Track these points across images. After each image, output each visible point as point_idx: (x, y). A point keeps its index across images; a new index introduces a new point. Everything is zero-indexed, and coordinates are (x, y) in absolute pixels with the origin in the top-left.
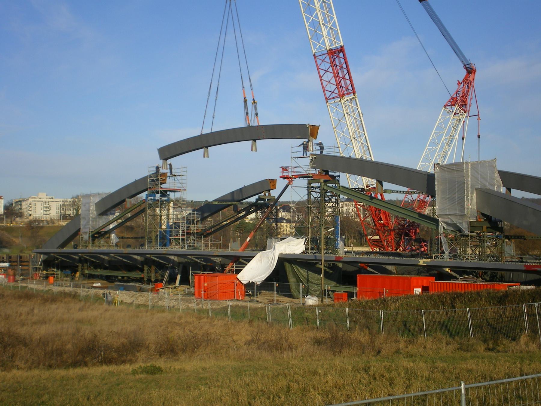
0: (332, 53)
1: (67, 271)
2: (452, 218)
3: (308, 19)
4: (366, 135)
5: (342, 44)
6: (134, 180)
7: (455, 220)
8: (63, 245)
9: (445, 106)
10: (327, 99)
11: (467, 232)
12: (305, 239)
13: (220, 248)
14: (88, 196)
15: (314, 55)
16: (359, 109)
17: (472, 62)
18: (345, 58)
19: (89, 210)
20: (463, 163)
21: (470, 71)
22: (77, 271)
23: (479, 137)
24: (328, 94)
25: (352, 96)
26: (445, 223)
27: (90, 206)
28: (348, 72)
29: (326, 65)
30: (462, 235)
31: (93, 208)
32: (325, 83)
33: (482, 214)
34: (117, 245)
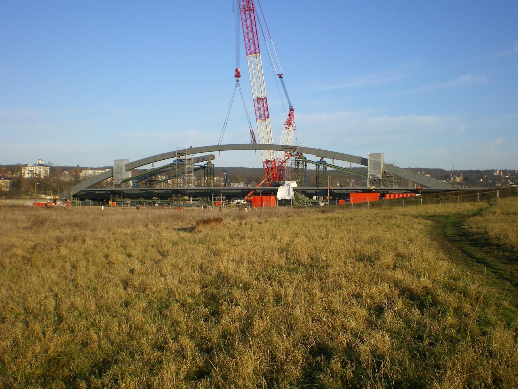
0: (258, 99)
1: (87, 200)
2: (374, 173)
3: (252, 82)
4: (272, 137)
5: (266, 96)
6: (161, 153)
7: (376, 174)
8: (88, 188)
9: (284, 124)
10: (257, 120)
11: (381, 178)
12: (296, 182)
13: (212, 186)
14: (122, 160)
15: (254, 100)
16: (270, 126)
17: (293, 106)
18: (266, 102)
19: (122, 169)
20: (380, 154)
21: (292, 110)
22: (110, 200)
23: (296, 139)
24: (258, 118)
25: (267, 120)
26: (371, 175)
27: (122, 166)
28: (267, 108)
29: (256, 105)
30: (378, 179)
31: (124, 167)
32: (256, 112)
33: (384, 172)
34: (132, 187)
